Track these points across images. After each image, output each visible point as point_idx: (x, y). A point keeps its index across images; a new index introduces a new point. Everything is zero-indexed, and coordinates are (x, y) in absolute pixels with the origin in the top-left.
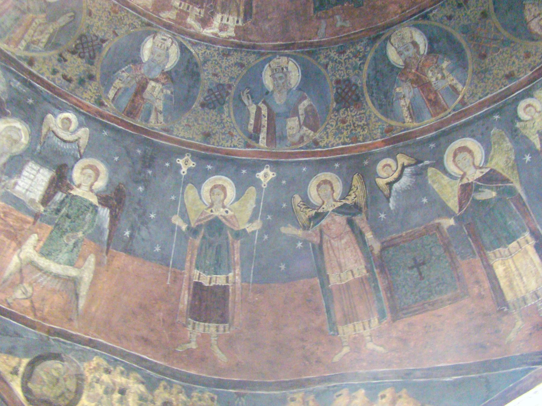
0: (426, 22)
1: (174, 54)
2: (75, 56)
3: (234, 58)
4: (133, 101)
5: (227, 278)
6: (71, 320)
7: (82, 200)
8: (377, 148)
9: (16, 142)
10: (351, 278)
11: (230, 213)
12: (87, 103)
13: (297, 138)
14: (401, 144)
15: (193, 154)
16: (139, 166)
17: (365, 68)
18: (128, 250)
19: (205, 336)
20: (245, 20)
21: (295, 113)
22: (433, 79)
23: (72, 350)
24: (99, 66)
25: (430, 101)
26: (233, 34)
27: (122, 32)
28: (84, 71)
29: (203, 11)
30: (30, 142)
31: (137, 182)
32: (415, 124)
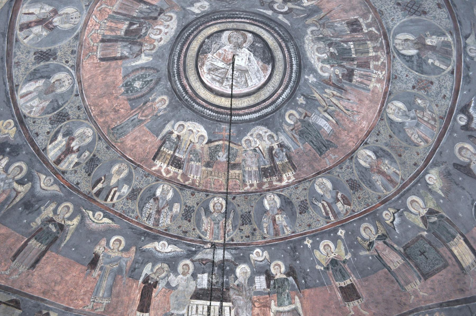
0: (368, 146)
1: (276, 198)
2: (244, 226)
3: (301, 187)
4: (274, 228)
5: (350, 280)
7: (280, 279)
8: (378, 207)
9: (246, 273)
10: (399, 265)
11: (337, 254)
12: (260, 241)
13: (345, 211)
14: (387, 203)
15: (309, 237)
16: (292, 254)
17: (355, 171)
18: (308, 287)
19: (355, 307)
20: (295, 171)
21: (338, 200)
22: (385, 170)
24: (254, 223)
25: (389, 180)
26: (294, 179)
27: (253, 204)
28: (251, 229)
29: (277, 177)
30: (251, 270)
31: (295, 260)
32: (388, 193)
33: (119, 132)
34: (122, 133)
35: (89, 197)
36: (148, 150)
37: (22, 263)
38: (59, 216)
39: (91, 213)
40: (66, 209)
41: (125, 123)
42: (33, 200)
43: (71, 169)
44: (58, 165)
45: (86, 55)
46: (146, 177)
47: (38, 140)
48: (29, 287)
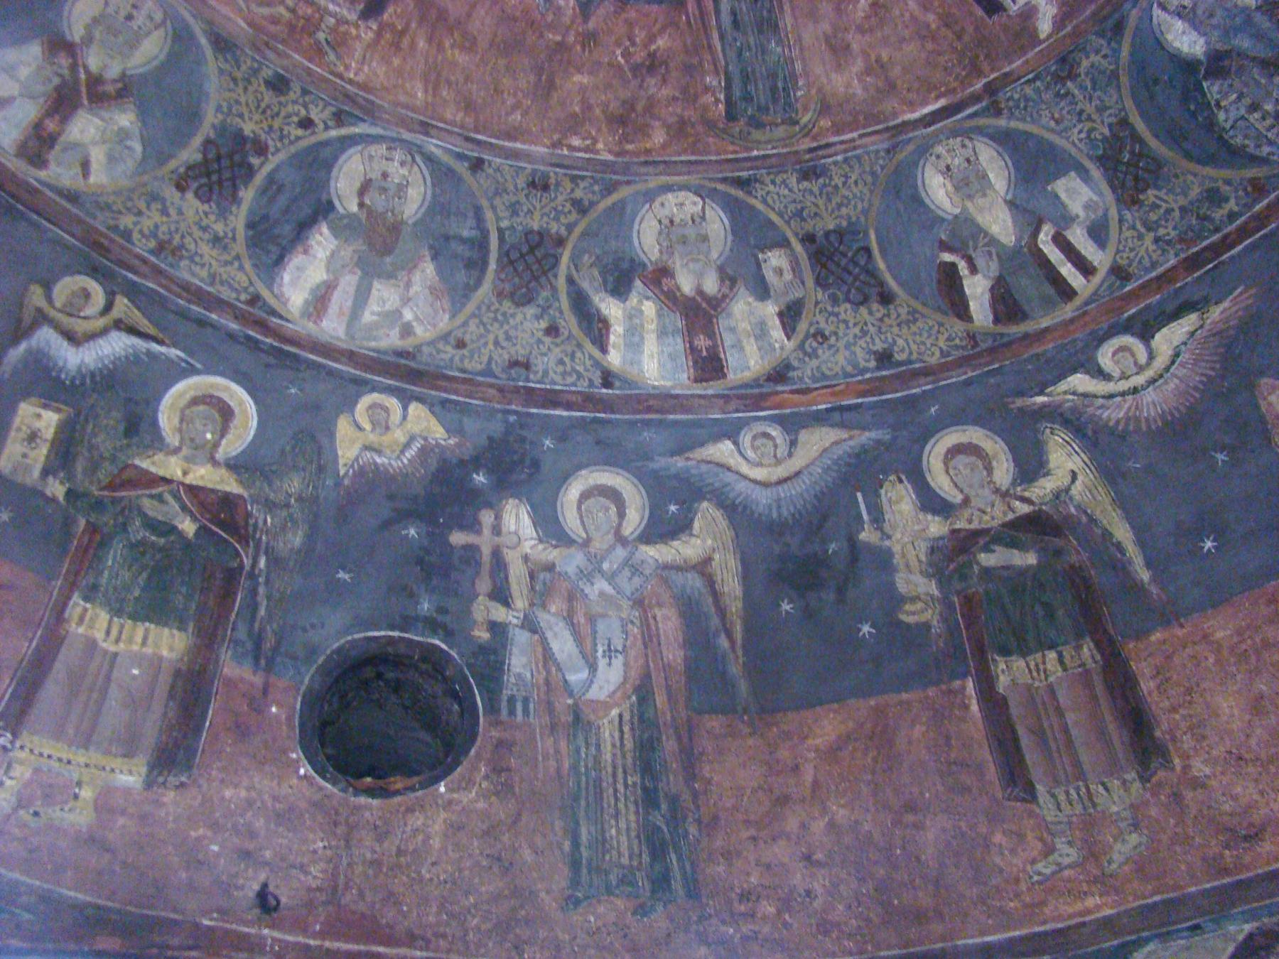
33: (762, 96)
34: (774, 89)
35: (992, 350)
36: (931, 17)
37: (1081, 776)
38: (976, 502)
39: (1080, 382)
40: (961, 460)
41: (732, 55)
42: (794, 542)
43: (790, 345)
44: (724, 376)
45: (320, 52)
46: (1072, 76)
47: (546, 373)
48: (1254, 836)
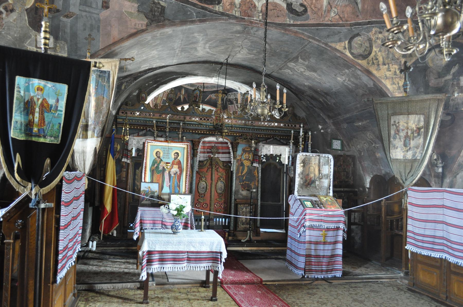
6: (358, 16)
23: (363, 29)
